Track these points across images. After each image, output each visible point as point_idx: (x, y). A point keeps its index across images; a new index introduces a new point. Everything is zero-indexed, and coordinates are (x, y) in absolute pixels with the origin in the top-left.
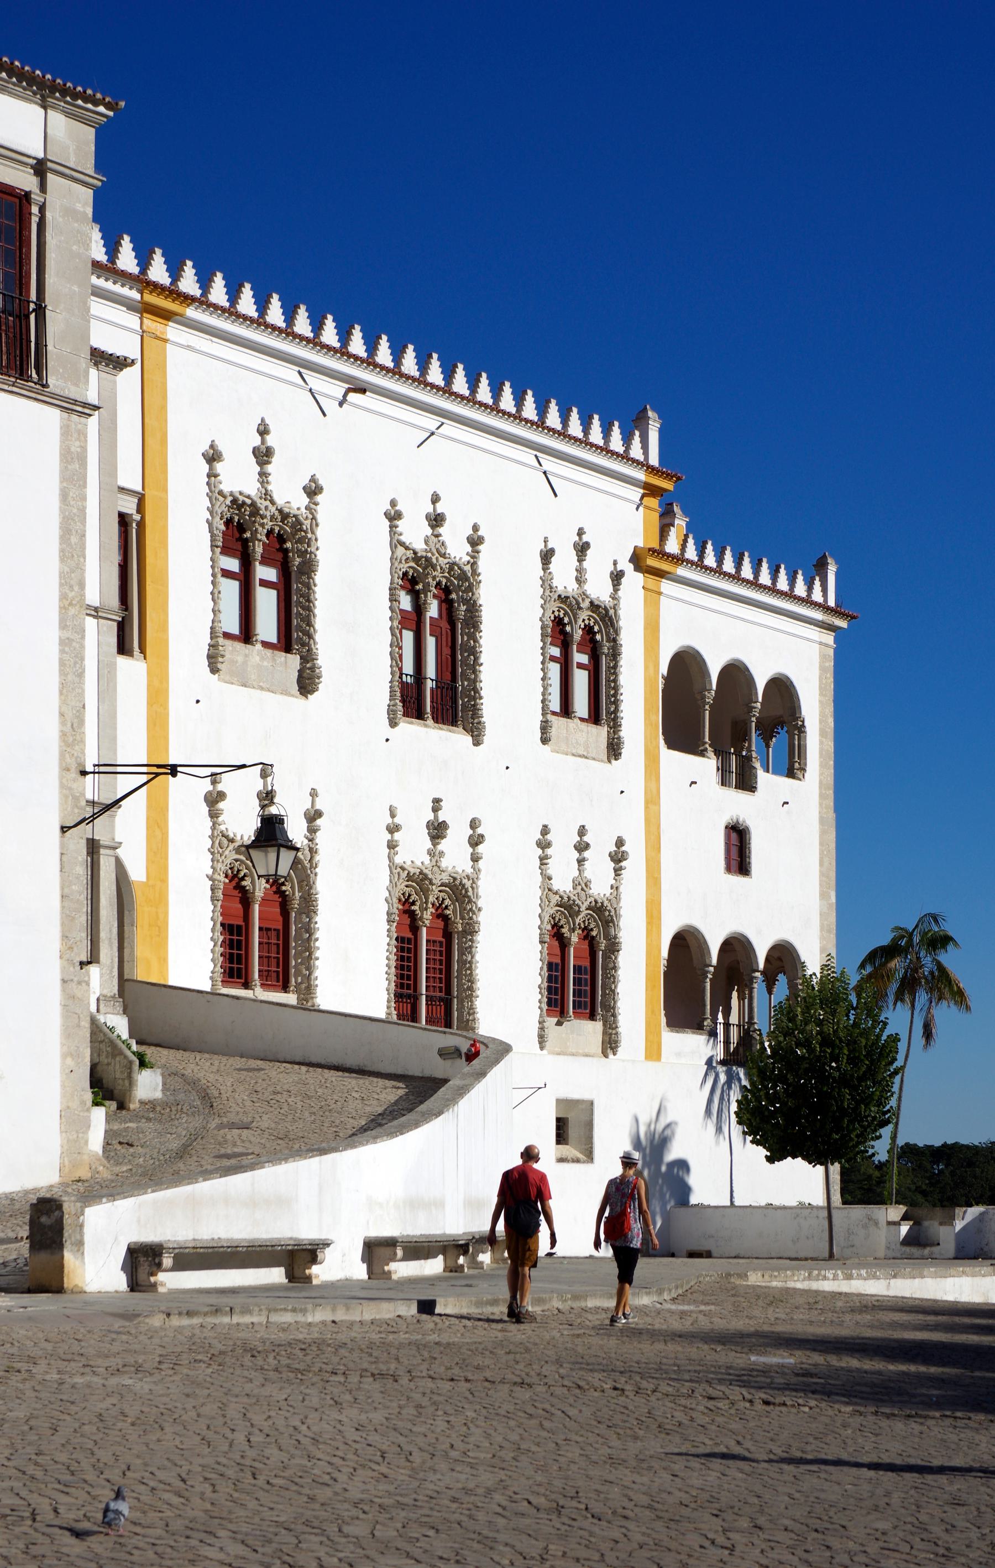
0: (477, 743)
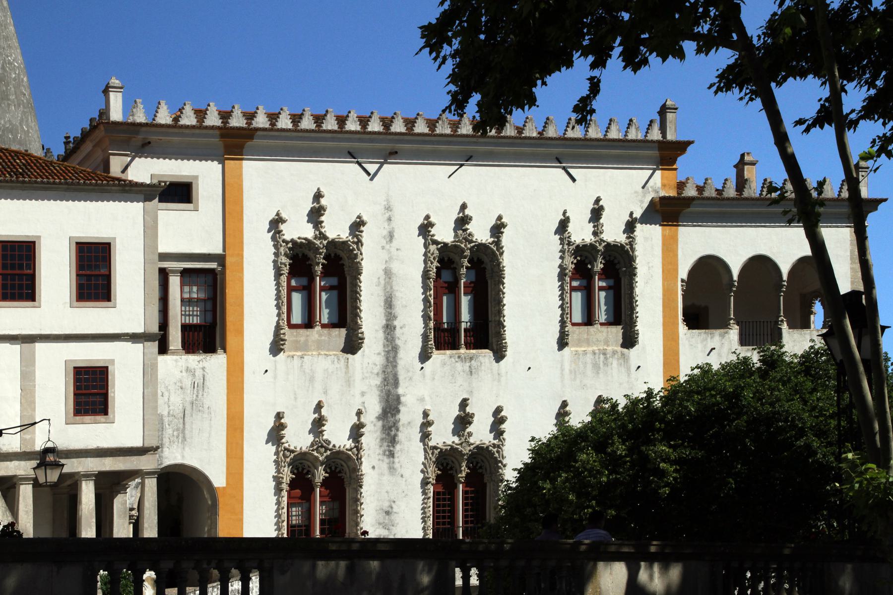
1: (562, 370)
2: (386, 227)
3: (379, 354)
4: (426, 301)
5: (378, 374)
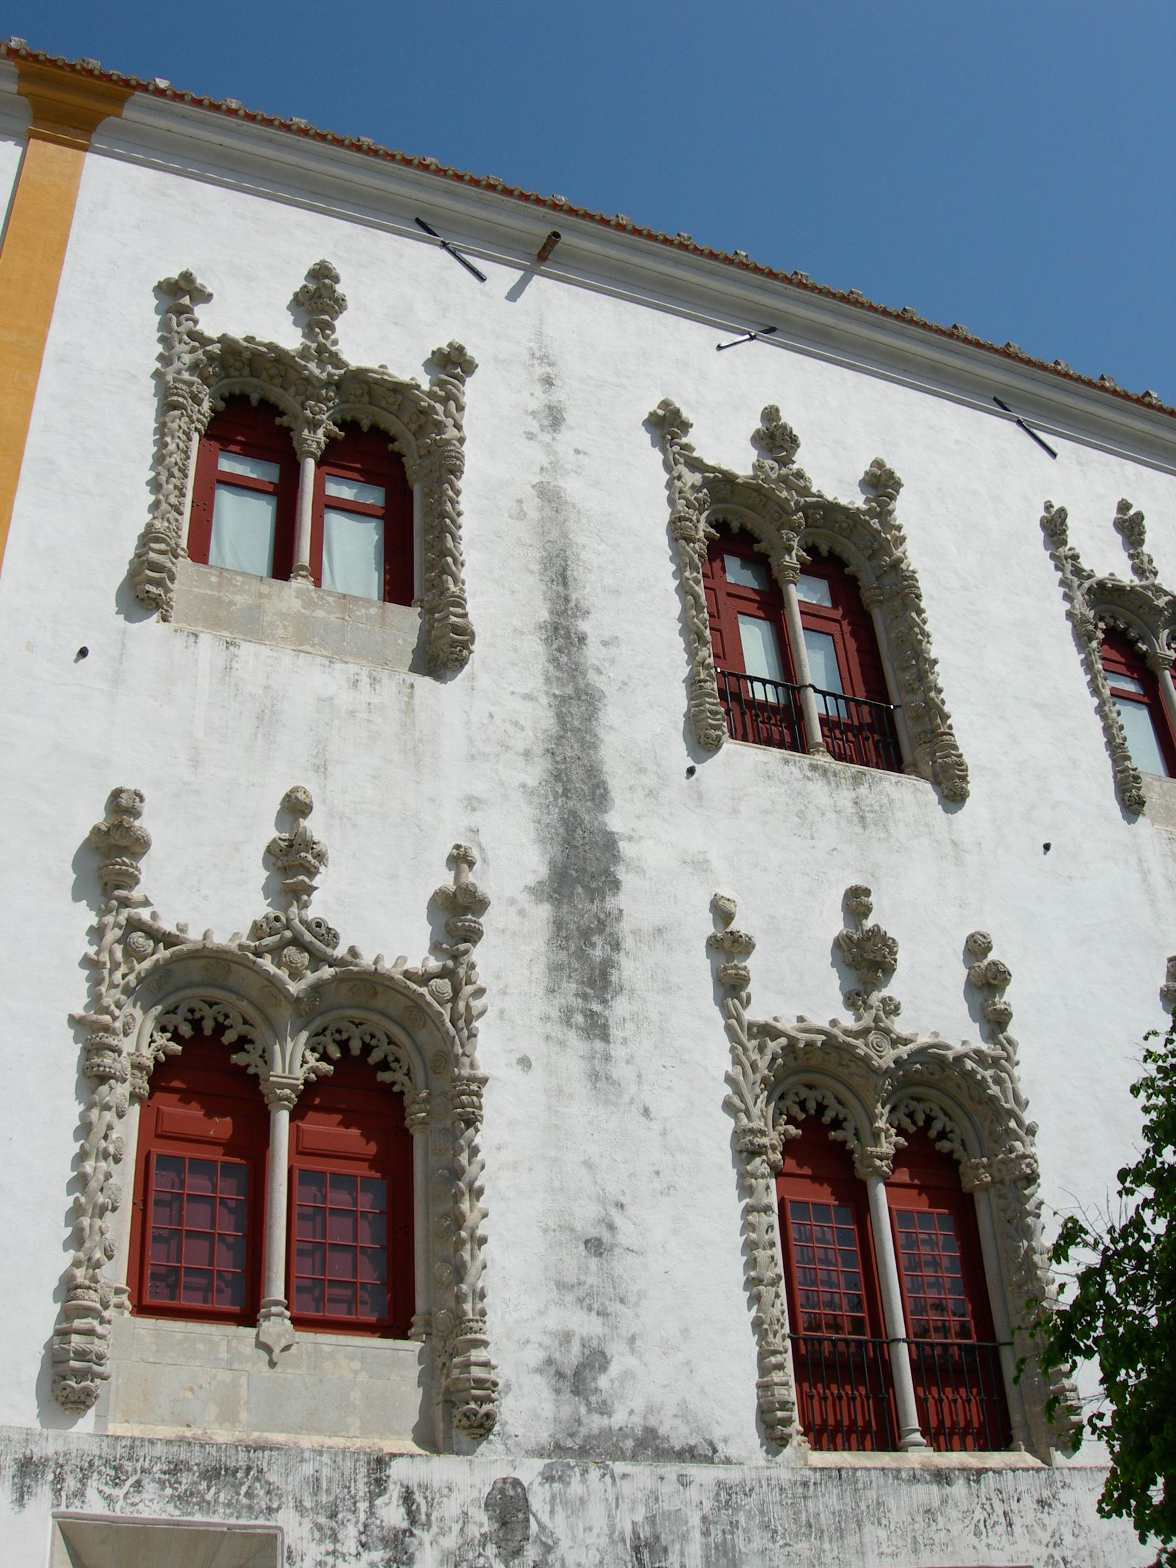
0: (953, 793)
1: (1145, 874)
3: (528, 697)
4: (684, 590)
5: (527, 754)
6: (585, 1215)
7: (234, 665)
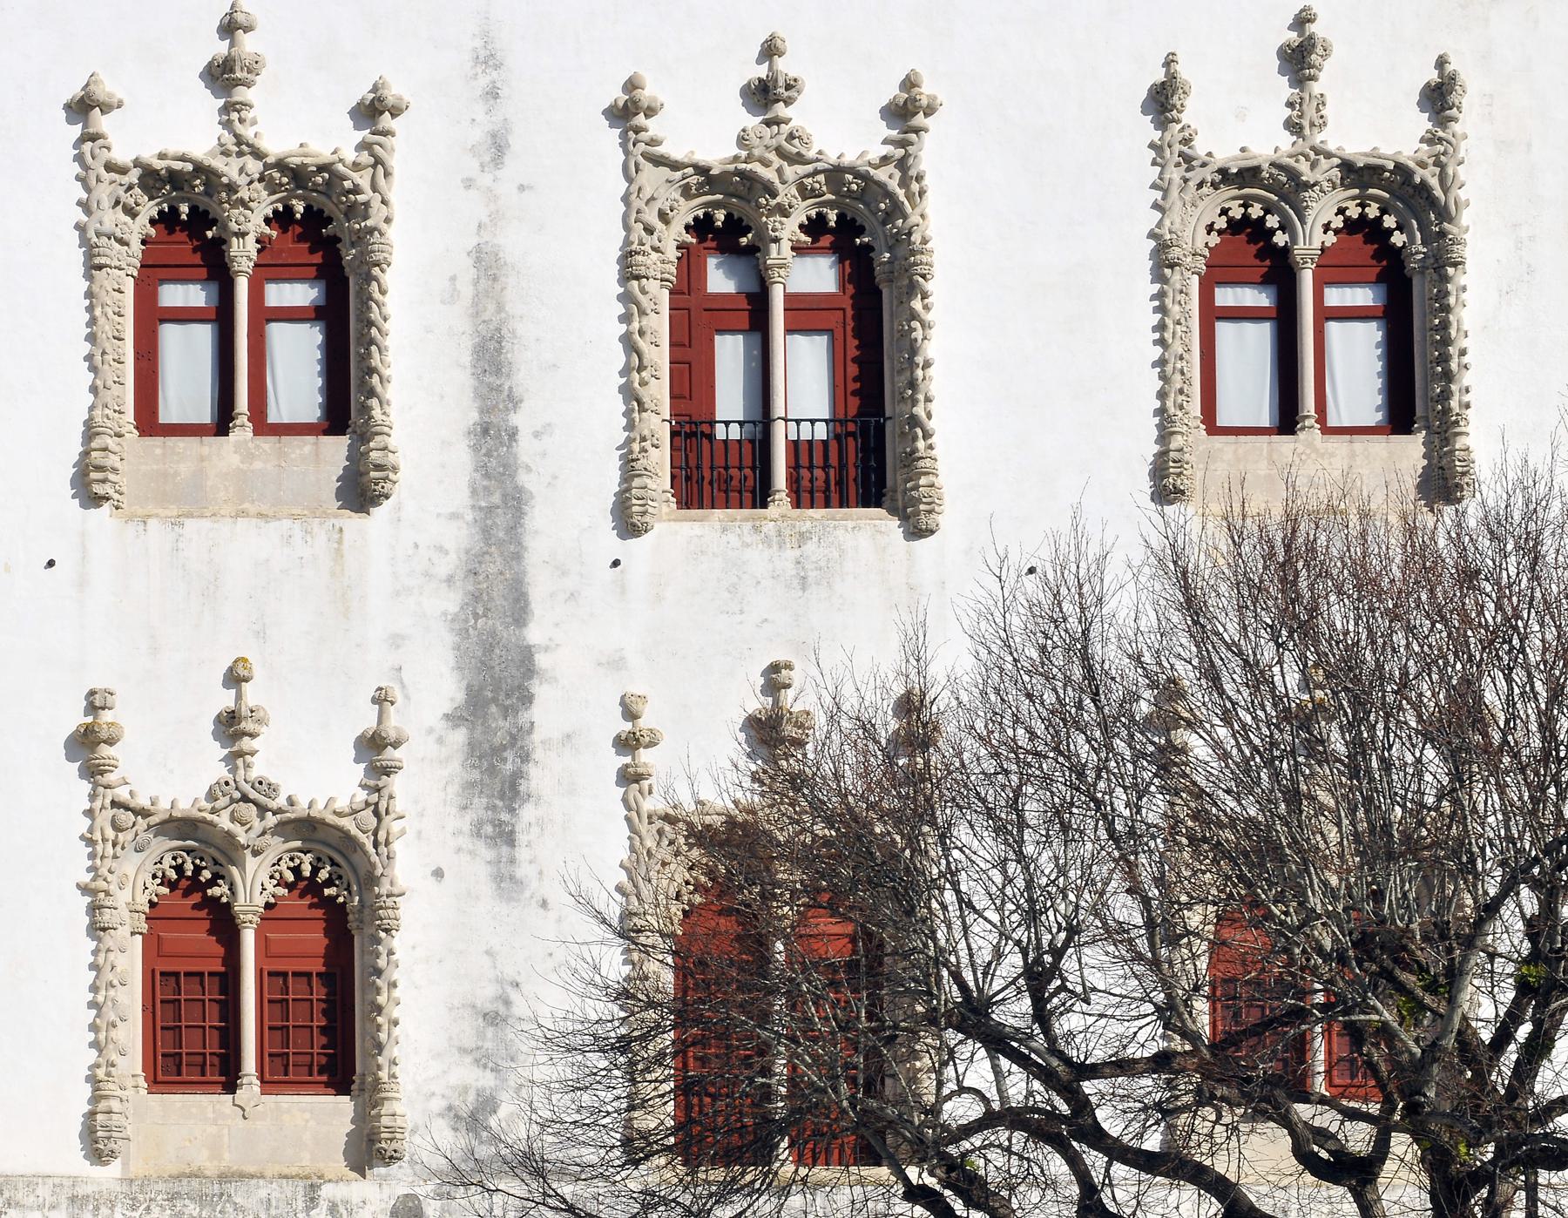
2: (480, 116)
3: (454, 516)
5: (450, 580)
6: (485, 994)
7: (181, 545)
